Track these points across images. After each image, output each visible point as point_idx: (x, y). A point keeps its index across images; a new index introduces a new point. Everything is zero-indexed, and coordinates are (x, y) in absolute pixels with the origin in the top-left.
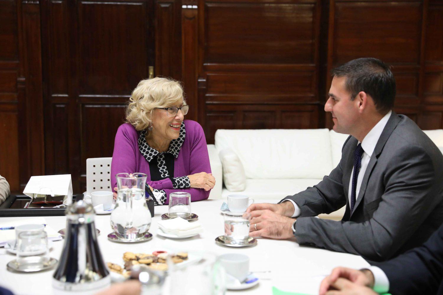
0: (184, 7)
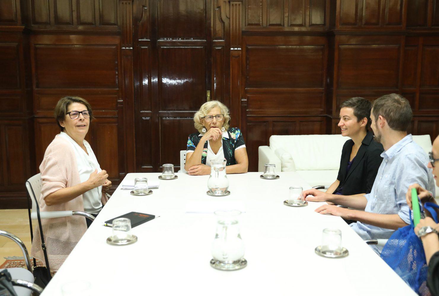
0: (232, 49)
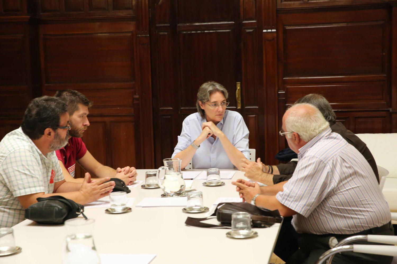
0: (265, 31)
